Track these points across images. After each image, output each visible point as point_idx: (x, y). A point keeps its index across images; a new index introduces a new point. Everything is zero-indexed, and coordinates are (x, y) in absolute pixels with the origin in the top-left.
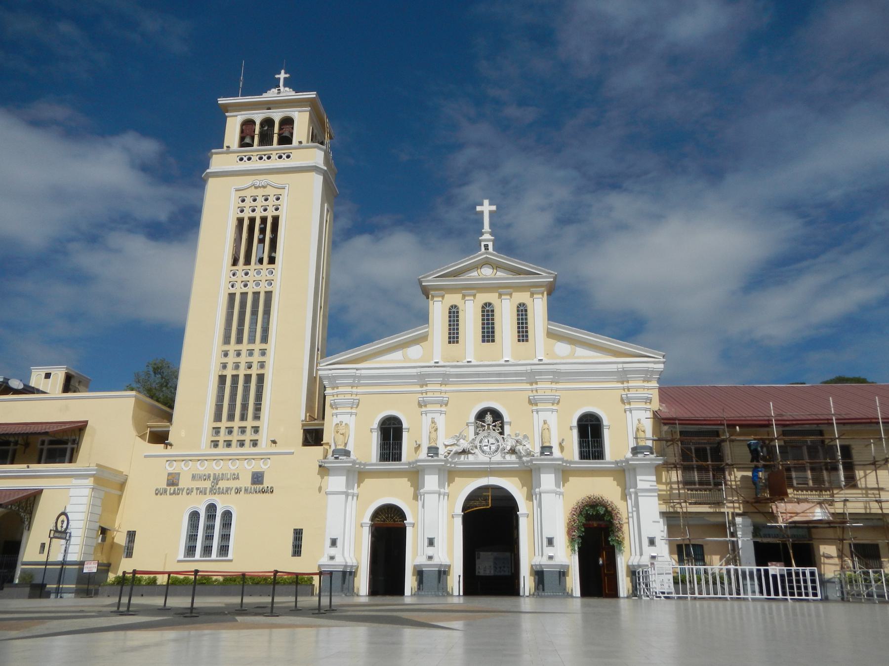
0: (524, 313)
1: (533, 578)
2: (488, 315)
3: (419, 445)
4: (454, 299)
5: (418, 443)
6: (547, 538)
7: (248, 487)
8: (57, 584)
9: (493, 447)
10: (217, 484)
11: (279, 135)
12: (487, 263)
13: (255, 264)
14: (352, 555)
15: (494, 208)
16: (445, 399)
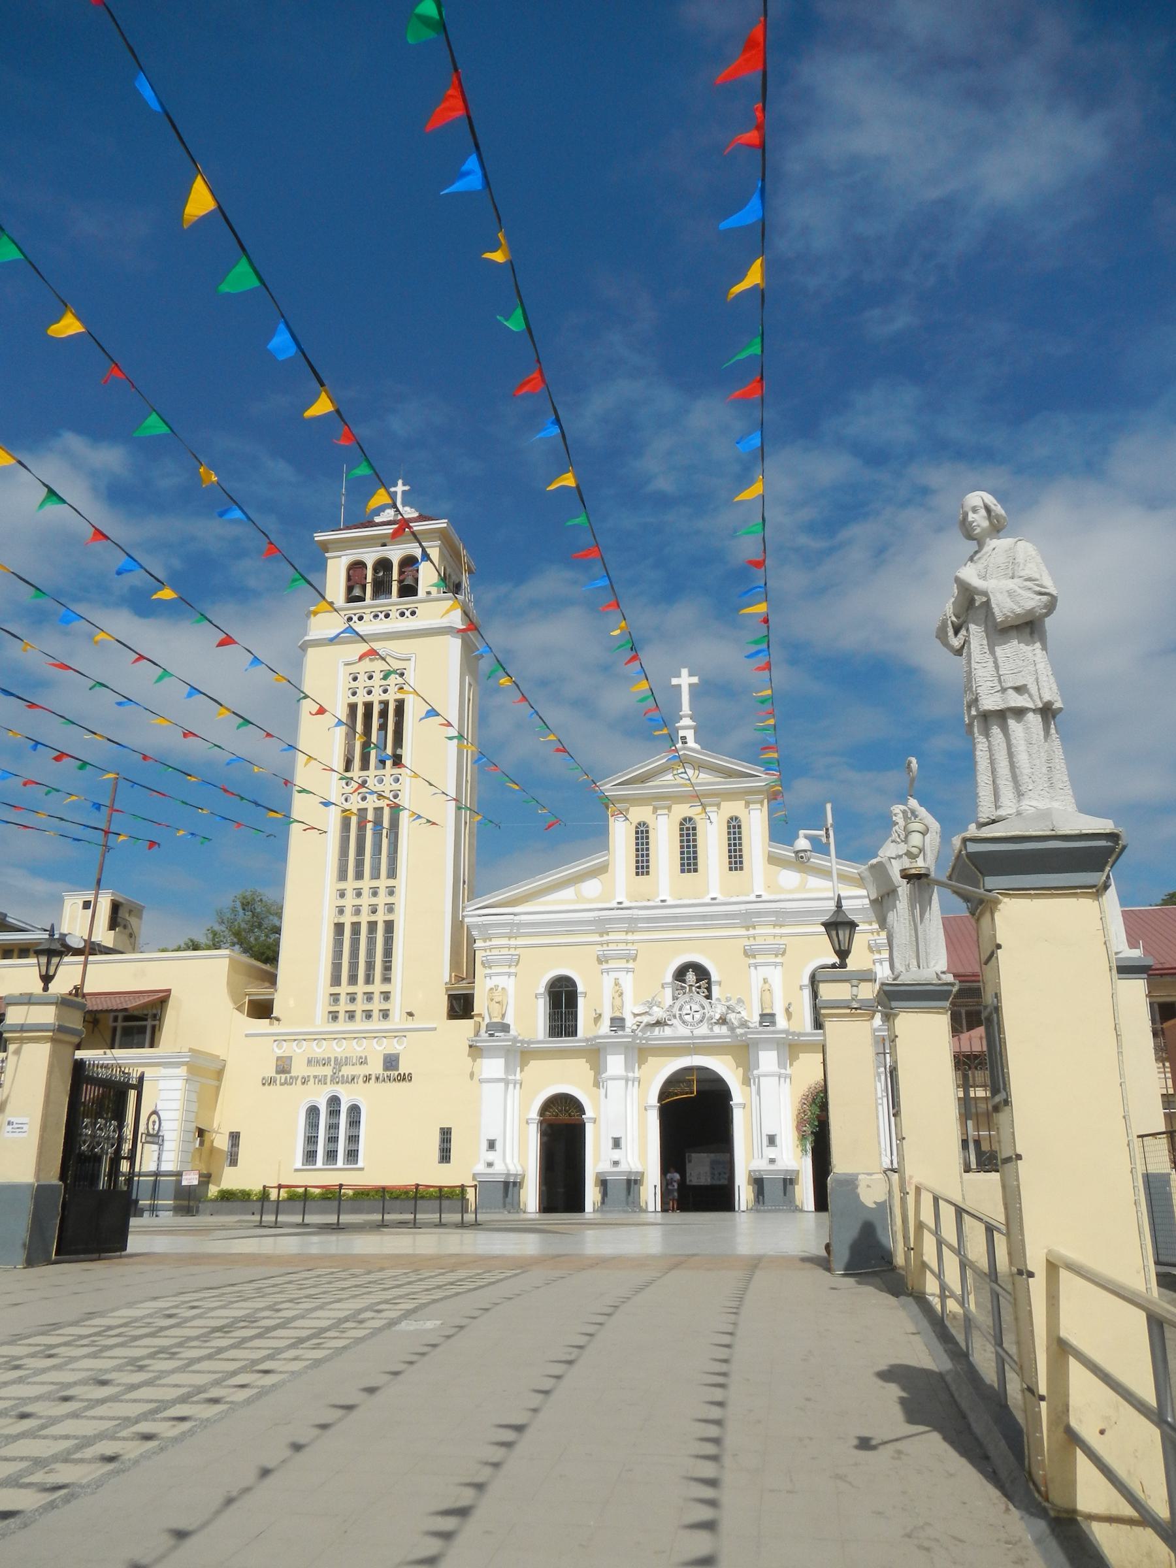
0: (737, 830)
1: (751, 1187)
2: (688, 835)
3: (600, 1015)
4: (639, 814)
5: (598, 1012)
6: (767, 1135)
7: (379, 1074)
8: (151, 1199)
9: (698, 1016)
10: (340, 1071)
11: (400, 581)
13: (376, 768)
14: (516, 1161)
15: (695, 680)
16: (632, 952)
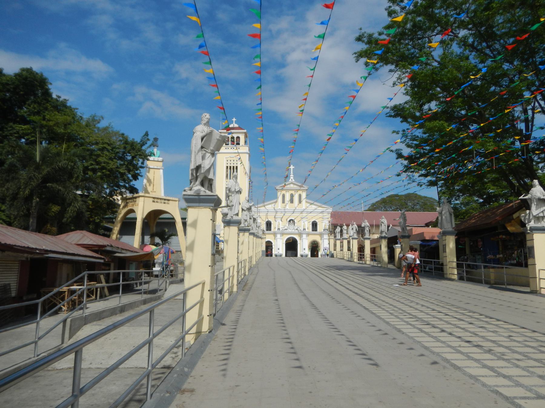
4: (284, 192)
11: (236, 141)
12: (292, 183)
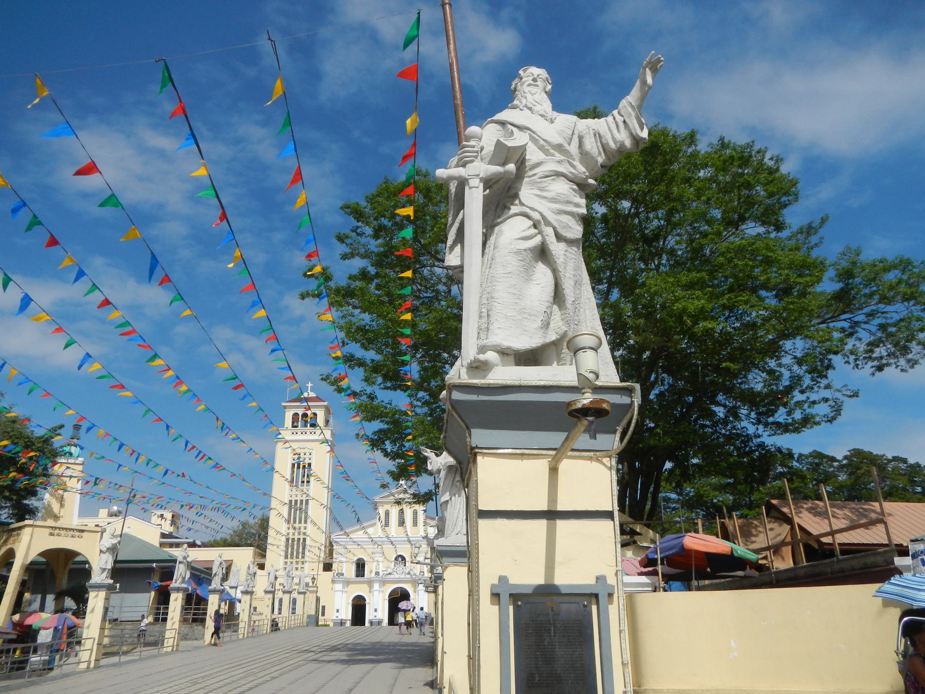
9: (401, 572)
